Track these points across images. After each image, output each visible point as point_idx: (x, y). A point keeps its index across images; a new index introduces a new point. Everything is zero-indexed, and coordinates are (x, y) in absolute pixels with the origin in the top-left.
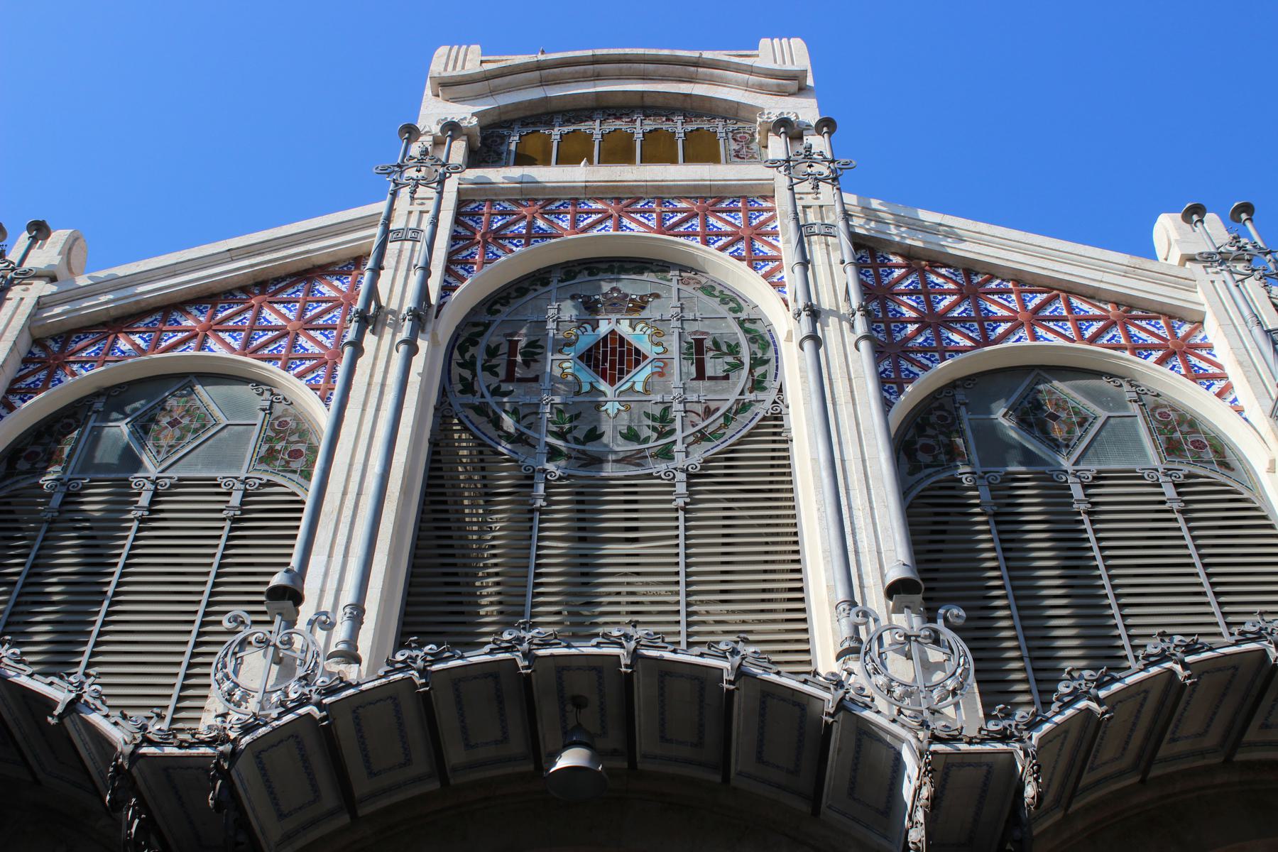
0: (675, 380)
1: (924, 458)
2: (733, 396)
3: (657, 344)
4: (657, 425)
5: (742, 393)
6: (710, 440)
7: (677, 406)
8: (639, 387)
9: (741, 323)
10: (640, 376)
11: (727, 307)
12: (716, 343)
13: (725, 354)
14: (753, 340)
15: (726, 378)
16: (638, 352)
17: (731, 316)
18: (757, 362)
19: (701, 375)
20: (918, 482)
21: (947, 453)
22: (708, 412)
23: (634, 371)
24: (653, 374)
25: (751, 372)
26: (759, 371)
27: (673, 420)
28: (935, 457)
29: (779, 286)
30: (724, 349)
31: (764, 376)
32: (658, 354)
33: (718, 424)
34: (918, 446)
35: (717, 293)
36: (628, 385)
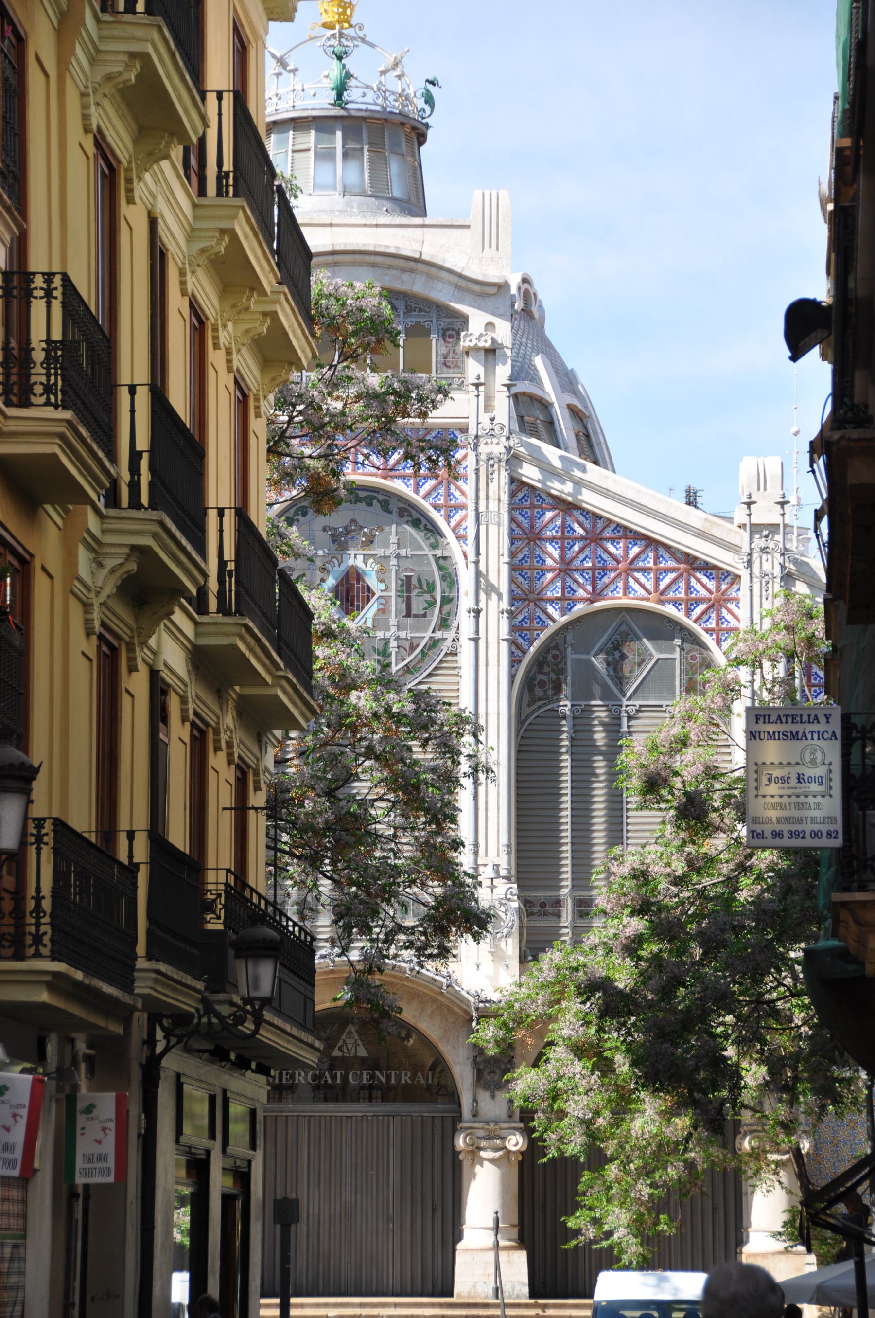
0: (393, 621)
1: (539, 692)
2: (429, 634)
3: (381, 581)
4: (380, 658)
5: (433, 632)
6: (412, 673)
7: (393, 643)
8: (369, 624)
9: (437, 559)
10: (371, 610)
11: (428, 542)
12: (419, 580)
13: (425, 592)
14: (443, 578)
15: (425, 615)
16: (369, 588)
17: (429, 553)
18: (446, 600)
19: (408, 614)
20: (532, 712)
21: (554, 688)
22: (413, 648)
23: (367, 608)
24: (378, 610)
25: (440, 611)
26: (446, 608)
27: (390, 654)
28: (545, 691)
29: (461, 538)
30: (425, 587)
31: (449, 614)
32: (382, 591)
33: (417, 659)
34: (536, 682)
35: (422, 526)
36: (363, 620)
